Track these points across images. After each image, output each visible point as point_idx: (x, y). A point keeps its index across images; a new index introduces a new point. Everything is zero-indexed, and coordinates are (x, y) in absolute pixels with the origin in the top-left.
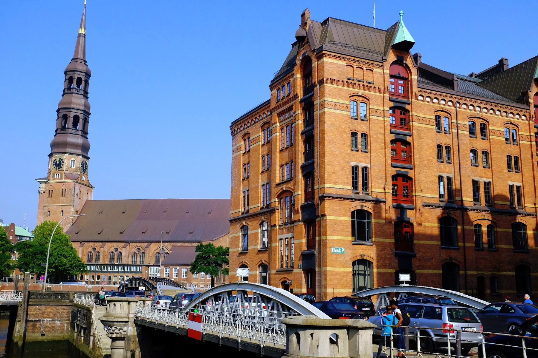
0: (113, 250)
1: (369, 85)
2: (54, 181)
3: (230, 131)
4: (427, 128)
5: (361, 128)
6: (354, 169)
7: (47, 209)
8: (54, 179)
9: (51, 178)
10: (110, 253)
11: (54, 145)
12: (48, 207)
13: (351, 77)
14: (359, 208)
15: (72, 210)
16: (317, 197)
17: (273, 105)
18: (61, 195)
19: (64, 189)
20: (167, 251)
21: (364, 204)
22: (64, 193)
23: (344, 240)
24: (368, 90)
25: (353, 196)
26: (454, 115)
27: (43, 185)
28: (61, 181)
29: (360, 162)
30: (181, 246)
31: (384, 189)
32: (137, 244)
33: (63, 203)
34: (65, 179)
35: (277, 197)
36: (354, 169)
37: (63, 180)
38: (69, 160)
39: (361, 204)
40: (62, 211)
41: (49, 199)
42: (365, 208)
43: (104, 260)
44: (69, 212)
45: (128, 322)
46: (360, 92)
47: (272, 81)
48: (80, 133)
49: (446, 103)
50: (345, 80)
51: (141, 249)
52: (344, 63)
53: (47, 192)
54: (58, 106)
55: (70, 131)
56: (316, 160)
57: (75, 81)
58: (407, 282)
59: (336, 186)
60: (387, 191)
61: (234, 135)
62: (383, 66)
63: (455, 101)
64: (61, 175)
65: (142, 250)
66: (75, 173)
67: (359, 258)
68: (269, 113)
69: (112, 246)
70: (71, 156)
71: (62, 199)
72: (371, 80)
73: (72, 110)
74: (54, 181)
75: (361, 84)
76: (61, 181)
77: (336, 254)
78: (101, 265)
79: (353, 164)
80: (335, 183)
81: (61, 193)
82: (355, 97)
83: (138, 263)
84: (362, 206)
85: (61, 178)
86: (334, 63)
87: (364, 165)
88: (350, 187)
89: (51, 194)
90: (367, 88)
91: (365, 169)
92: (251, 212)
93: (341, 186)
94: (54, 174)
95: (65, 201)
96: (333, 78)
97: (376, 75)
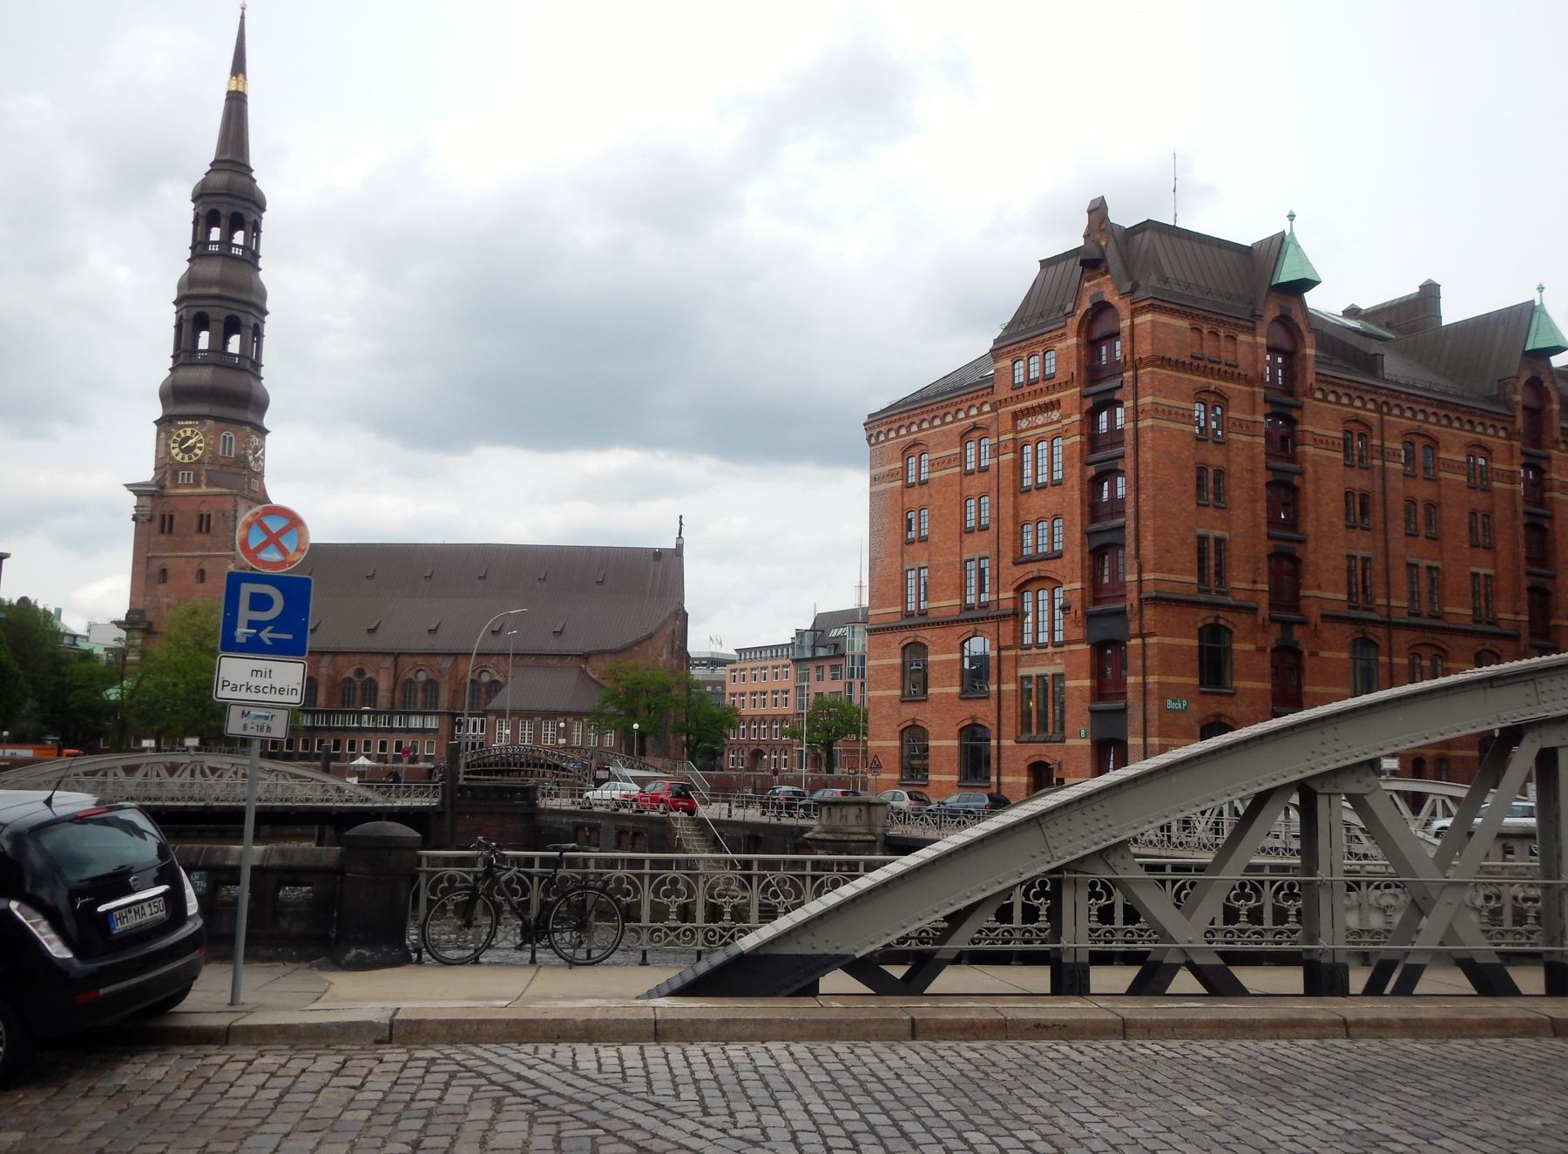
0: (350, 673)
1: (1230, 370)
3: (864, 435)
4: (1328, 458)
5: (1215, 458)
6: (1202, 539)
7: (156, 565)
8: (177, 486)
9: (168, 483)
11: (173, 394)
13: (1196, 351)
14: (1211, 621)
16: (1132, 596)
17: (1003, 392)
18: (195, 527)
21: (1221, 614)
22: (204, 524)
23: (1187, 685)
24: (1225, 379)
25: (1202, 598)
26: (1376, 431)
27: (147, 501)
28: (197, 491)
29: (1213, 527)
31: (1255, 582)
32: (419, 660)
34: (208, 485)
35: (1016, 590)
36: (1202, 539)
37: (204, 489)
39: (1215, 613)
40: (202, 572)
41: (162, 538)
42: (1222, 622)
43: (329, 701)
45: (874, 842)
46: (1214, 384)
47: (996, 341)
48: (248, 365)
49: (1364, 404)
50: (1188, 361)
52: (1184, 324)
54: (179, 288)
56: (1131, 525)
57: (224, 221)
58: (1394, 773)
59: (1172, 577)
60: (1260, 587)
61: (877, 443)
62: (1254, 329)
63: (1380, 399)
67: (1211, 720)
68: (987, 408)
70: (222, 425)
71: (200, 538)
72: (1231, 359)
75: (1216, 367)
76: (197, 491)
77: (1174, 711)
78: (328, 713)
79: (1201, 531)
80: (1171, 571)
81: (195, 522)
82: (1203, 396)
83: (419, 707)
84: (1217, 617)
85: (197, 484)
86: (1169, 325)
87: (1218, 533)
88: (1195, 580)
90: (1225, 376)
91: (1219, 541)
92: (932, 616)
93: (1180, 578)
94: (175, 474)
96: (1168, 355)
97: (1241, 349)
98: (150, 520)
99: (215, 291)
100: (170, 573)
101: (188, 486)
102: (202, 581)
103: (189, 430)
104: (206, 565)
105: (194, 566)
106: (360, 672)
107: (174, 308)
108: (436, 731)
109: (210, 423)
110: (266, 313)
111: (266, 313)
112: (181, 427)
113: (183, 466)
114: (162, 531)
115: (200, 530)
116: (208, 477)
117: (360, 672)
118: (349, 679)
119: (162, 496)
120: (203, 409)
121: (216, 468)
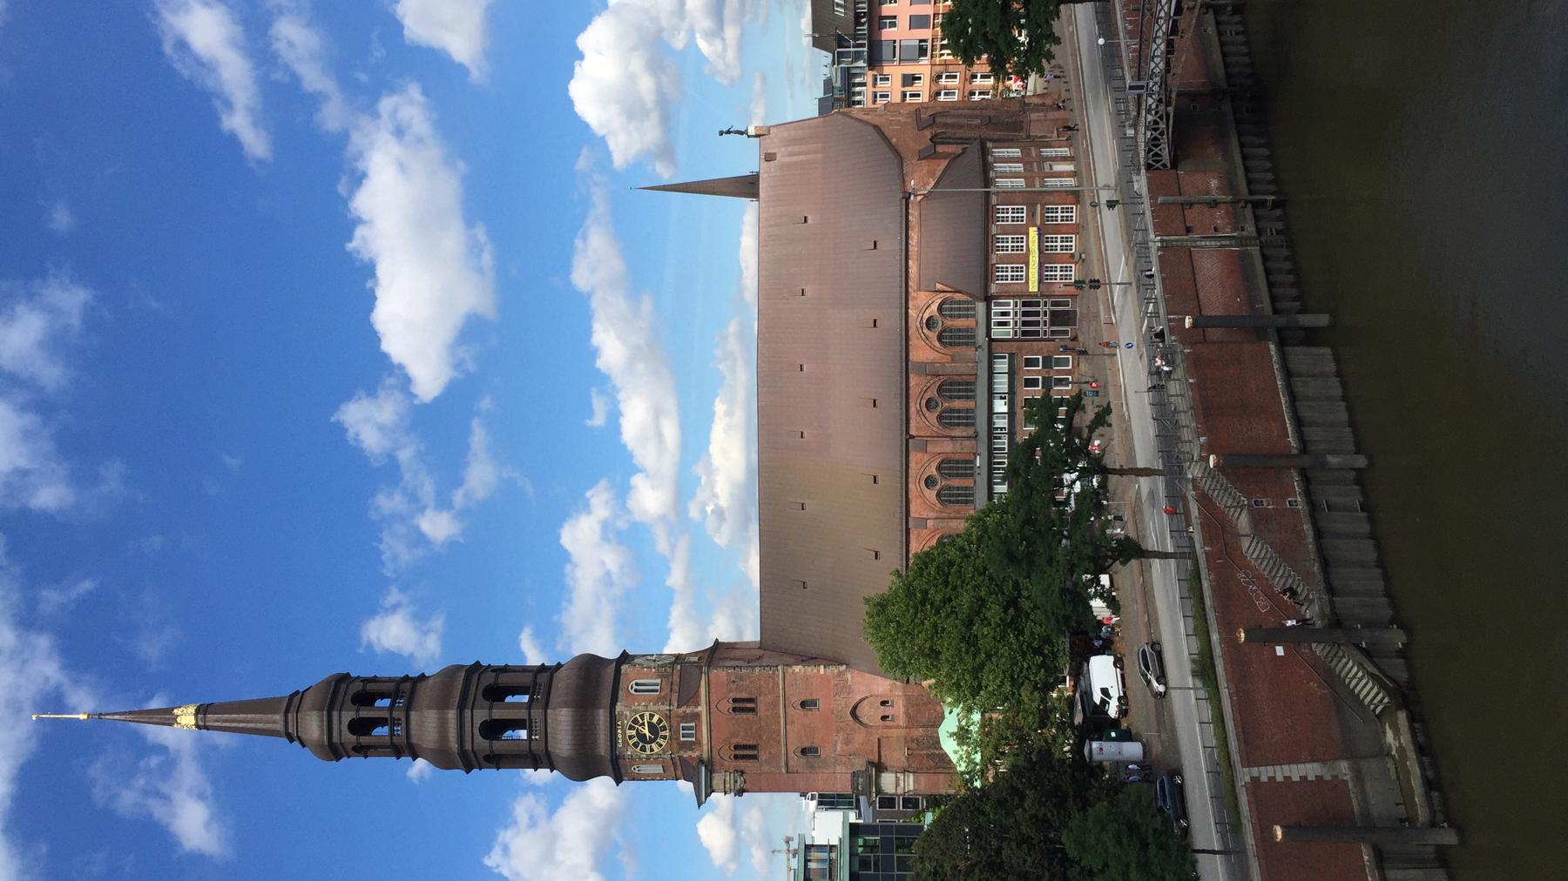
0: (931, 494)
2: (705, 741)
7: (796, 761)
8: (699, 743)
9: (695, 754)
10: (941, 502)
12: (791, 754)
15: (797, 669)
18: (750, 715)
19: (731, 705)
20: (935, 307)
22: (744, 705)
27: (718, 779)
28: (704, 718)
30: (919, 258)
32: (913, 410)
33: (775, 705)
34: (697, 704)
37: (702, 709)
38: (634, 698)
40: (803, 704)
41: (763, 756)
44: (807, 678)
51: (927, 396)
53: (742, 764)
55: (537, 714)
64: (685, 718)
65: (933, 393)
66: (676, 678)
69: (922, 495)
73: (468, 747)
74: (705, 741)
76: (704, 718)
89: (746, 752)
94: (684, 746)
95: (770, 698)
98: (742, 773)
99: (452, 715)
100: (807, 745)
101: (698, 728)
102: (814, 703)
103: (629, 732)
104: (796, 700)
105: (798, 712)
106: (930, 482)
107: (475, 771)
108: (1012, 356)
109: (619, 708)
110: (478, 663)
111: (478, 663)
112: (625, 743)
113: (674, 736)
114: (754, 757)
115: (752, 710)
116: (687, 704)
117: (930, 482)
118: (938, 495)
119: (711, 760)
120: (602, 716)
121: (675, 697)
